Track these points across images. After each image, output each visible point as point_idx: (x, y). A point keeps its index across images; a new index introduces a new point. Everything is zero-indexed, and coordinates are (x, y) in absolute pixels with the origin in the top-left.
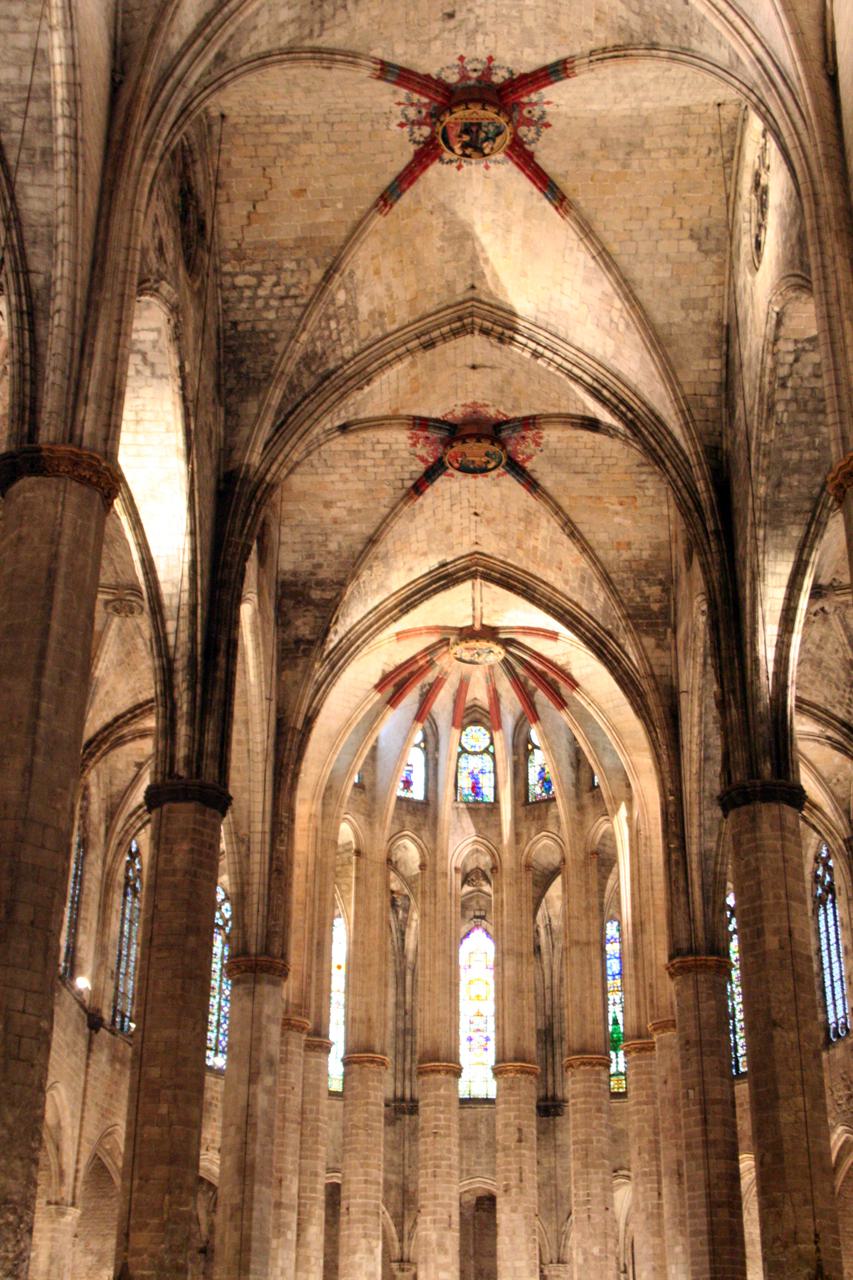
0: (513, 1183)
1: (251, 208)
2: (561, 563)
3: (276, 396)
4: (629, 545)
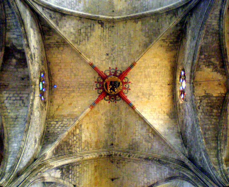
1: (58, 107)
3: (57, 143)
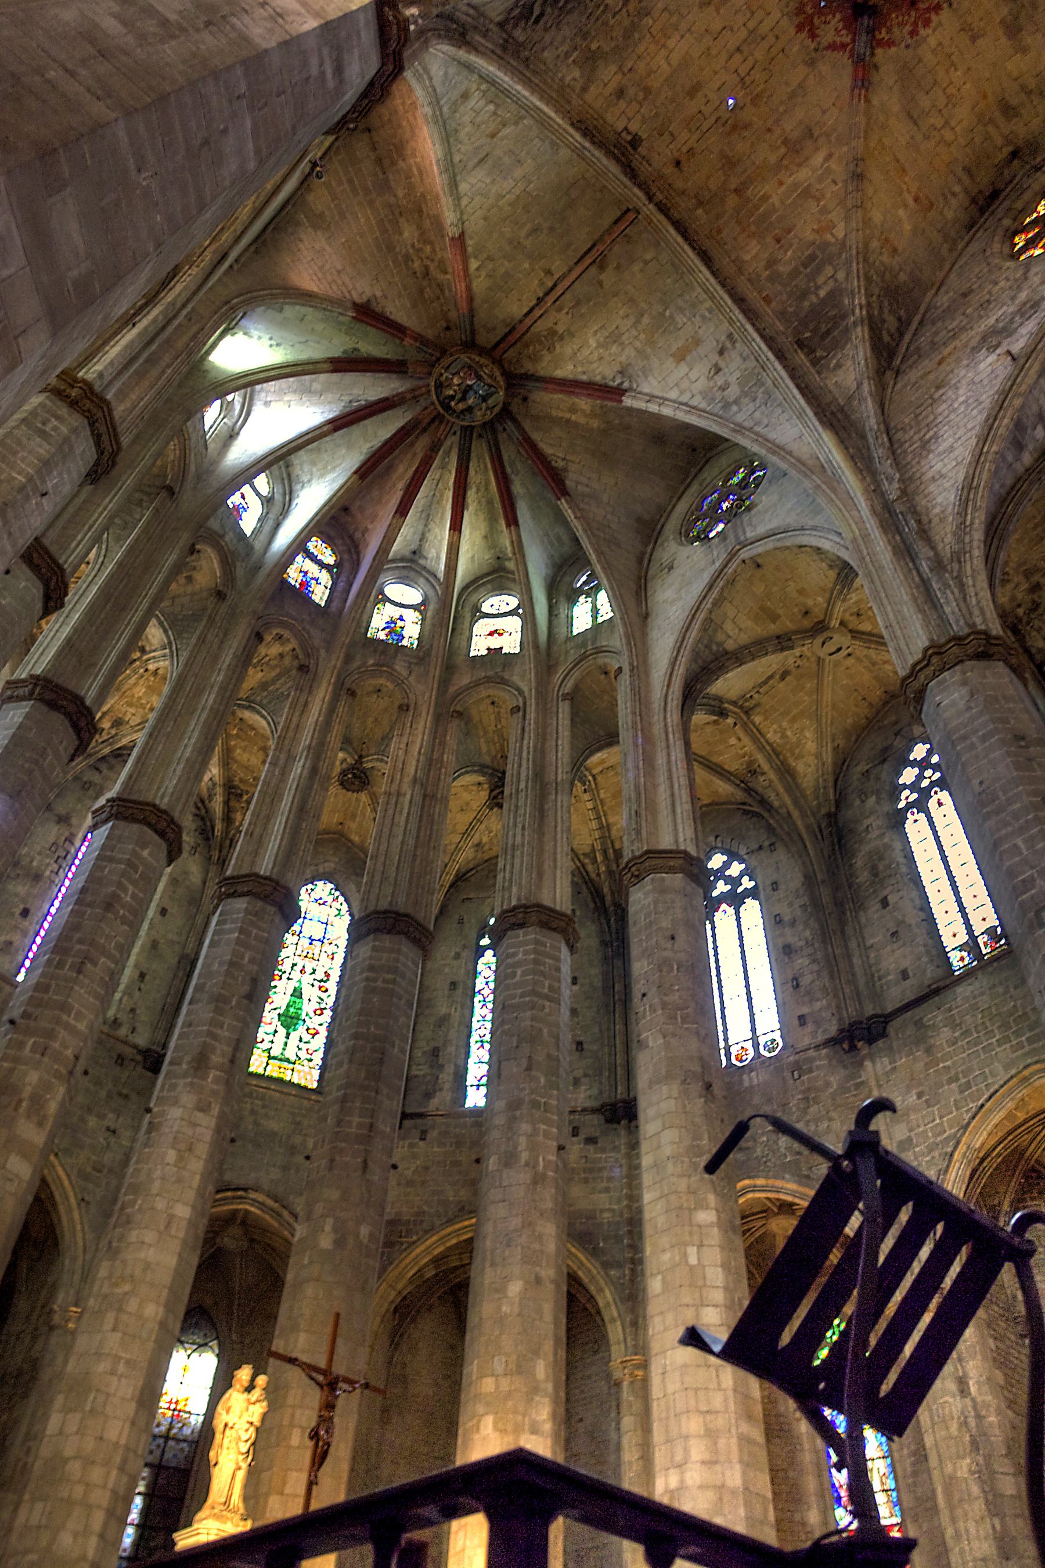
0: (216, 1059)
2: (790, 232)
4: (895, 251)
